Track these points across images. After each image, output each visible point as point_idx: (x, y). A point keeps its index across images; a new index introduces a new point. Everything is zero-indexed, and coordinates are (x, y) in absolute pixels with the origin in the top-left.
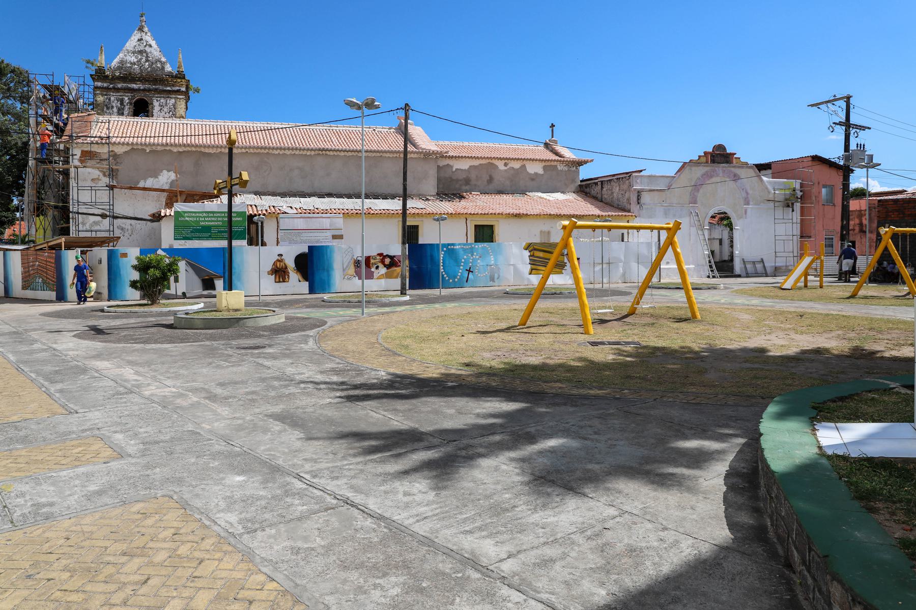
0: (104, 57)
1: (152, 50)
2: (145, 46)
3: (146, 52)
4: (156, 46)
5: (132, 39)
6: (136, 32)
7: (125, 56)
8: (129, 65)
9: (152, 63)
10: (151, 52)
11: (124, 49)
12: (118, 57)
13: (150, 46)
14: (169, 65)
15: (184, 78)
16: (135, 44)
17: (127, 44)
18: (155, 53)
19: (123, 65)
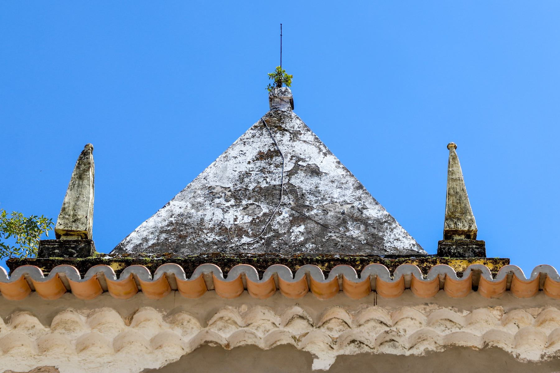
0: (90, 193)
1: (323, 185)
2: (290, 174)
3: (292, 190)
4: (341, 172)
5: (232, 152)
6: (249, 133)
7: (197, 206)
8: (211, 237)
9: (325, 227)
10: (316, 192)
11: (196, 185)
12: (163, 213)
13: (315, 172)
14: (399, 231)
15: (481, 254)
16: (244, 168)
17: (210, 171)
18: (336, 193)
19: (182, 237)
